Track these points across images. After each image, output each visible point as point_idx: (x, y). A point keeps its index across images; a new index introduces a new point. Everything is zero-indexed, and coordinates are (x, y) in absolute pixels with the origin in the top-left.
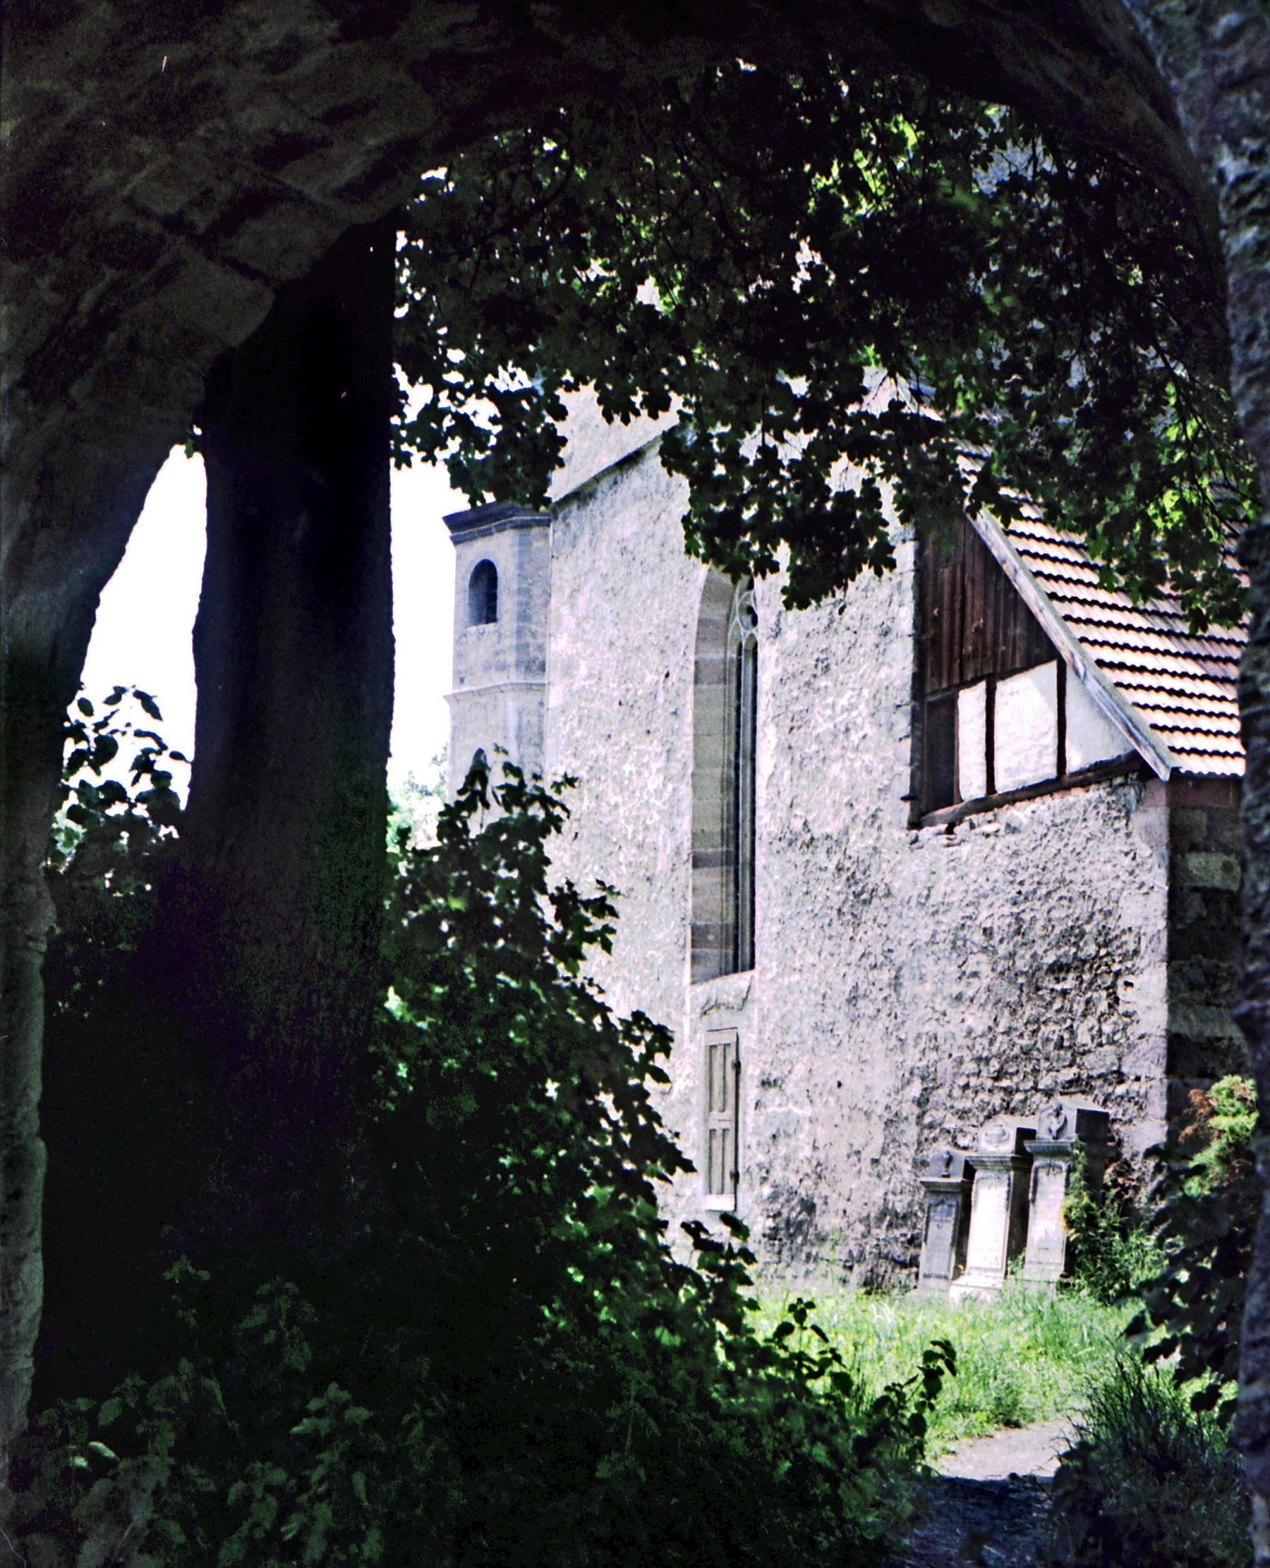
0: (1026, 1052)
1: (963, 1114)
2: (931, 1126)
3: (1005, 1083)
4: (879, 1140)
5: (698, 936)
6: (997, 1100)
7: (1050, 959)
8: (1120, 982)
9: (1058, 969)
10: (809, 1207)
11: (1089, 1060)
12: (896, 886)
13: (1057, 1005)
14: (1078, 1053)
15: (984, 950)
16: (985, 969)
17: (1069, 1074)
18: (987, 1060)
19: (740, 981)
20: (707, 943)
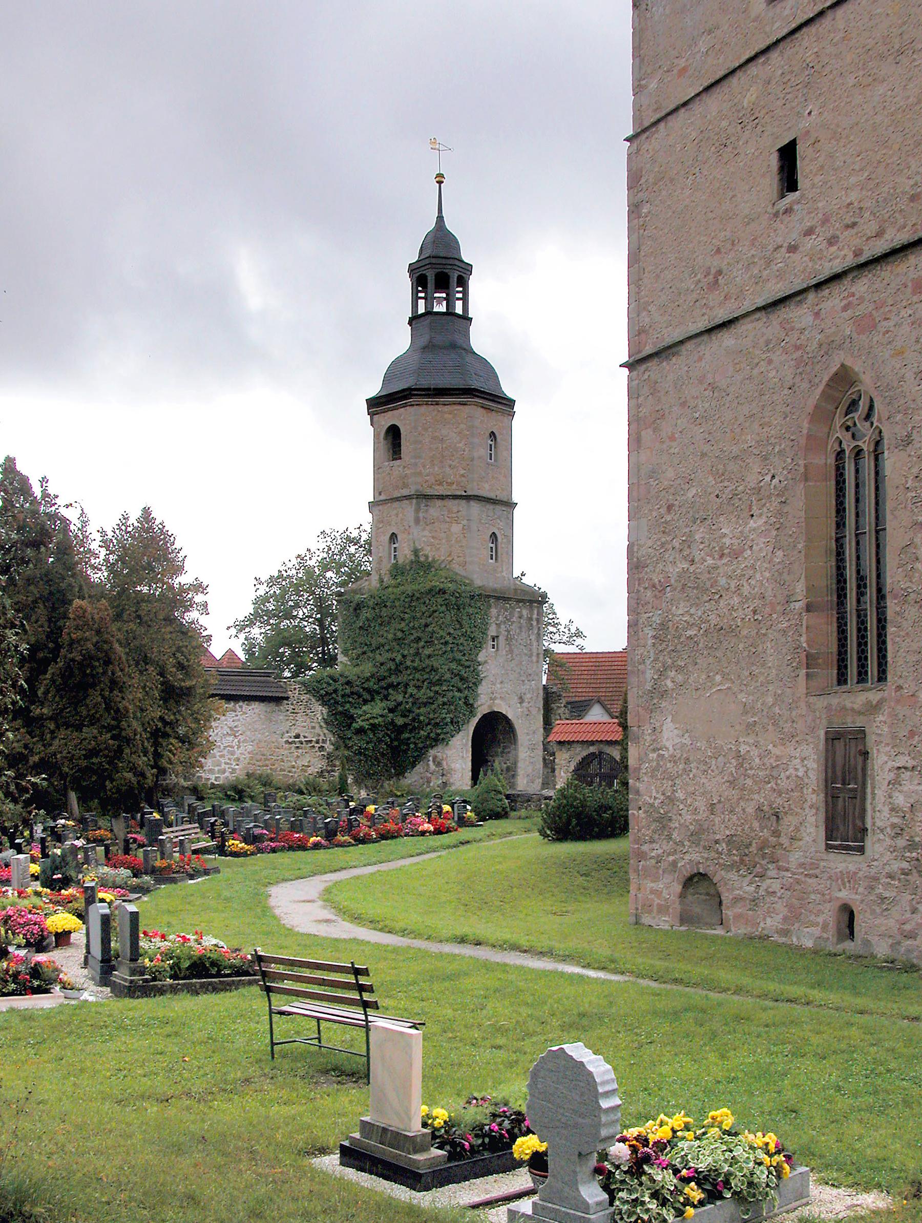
5: (811, 661)
19: (874, 696)
20: (817, 666)
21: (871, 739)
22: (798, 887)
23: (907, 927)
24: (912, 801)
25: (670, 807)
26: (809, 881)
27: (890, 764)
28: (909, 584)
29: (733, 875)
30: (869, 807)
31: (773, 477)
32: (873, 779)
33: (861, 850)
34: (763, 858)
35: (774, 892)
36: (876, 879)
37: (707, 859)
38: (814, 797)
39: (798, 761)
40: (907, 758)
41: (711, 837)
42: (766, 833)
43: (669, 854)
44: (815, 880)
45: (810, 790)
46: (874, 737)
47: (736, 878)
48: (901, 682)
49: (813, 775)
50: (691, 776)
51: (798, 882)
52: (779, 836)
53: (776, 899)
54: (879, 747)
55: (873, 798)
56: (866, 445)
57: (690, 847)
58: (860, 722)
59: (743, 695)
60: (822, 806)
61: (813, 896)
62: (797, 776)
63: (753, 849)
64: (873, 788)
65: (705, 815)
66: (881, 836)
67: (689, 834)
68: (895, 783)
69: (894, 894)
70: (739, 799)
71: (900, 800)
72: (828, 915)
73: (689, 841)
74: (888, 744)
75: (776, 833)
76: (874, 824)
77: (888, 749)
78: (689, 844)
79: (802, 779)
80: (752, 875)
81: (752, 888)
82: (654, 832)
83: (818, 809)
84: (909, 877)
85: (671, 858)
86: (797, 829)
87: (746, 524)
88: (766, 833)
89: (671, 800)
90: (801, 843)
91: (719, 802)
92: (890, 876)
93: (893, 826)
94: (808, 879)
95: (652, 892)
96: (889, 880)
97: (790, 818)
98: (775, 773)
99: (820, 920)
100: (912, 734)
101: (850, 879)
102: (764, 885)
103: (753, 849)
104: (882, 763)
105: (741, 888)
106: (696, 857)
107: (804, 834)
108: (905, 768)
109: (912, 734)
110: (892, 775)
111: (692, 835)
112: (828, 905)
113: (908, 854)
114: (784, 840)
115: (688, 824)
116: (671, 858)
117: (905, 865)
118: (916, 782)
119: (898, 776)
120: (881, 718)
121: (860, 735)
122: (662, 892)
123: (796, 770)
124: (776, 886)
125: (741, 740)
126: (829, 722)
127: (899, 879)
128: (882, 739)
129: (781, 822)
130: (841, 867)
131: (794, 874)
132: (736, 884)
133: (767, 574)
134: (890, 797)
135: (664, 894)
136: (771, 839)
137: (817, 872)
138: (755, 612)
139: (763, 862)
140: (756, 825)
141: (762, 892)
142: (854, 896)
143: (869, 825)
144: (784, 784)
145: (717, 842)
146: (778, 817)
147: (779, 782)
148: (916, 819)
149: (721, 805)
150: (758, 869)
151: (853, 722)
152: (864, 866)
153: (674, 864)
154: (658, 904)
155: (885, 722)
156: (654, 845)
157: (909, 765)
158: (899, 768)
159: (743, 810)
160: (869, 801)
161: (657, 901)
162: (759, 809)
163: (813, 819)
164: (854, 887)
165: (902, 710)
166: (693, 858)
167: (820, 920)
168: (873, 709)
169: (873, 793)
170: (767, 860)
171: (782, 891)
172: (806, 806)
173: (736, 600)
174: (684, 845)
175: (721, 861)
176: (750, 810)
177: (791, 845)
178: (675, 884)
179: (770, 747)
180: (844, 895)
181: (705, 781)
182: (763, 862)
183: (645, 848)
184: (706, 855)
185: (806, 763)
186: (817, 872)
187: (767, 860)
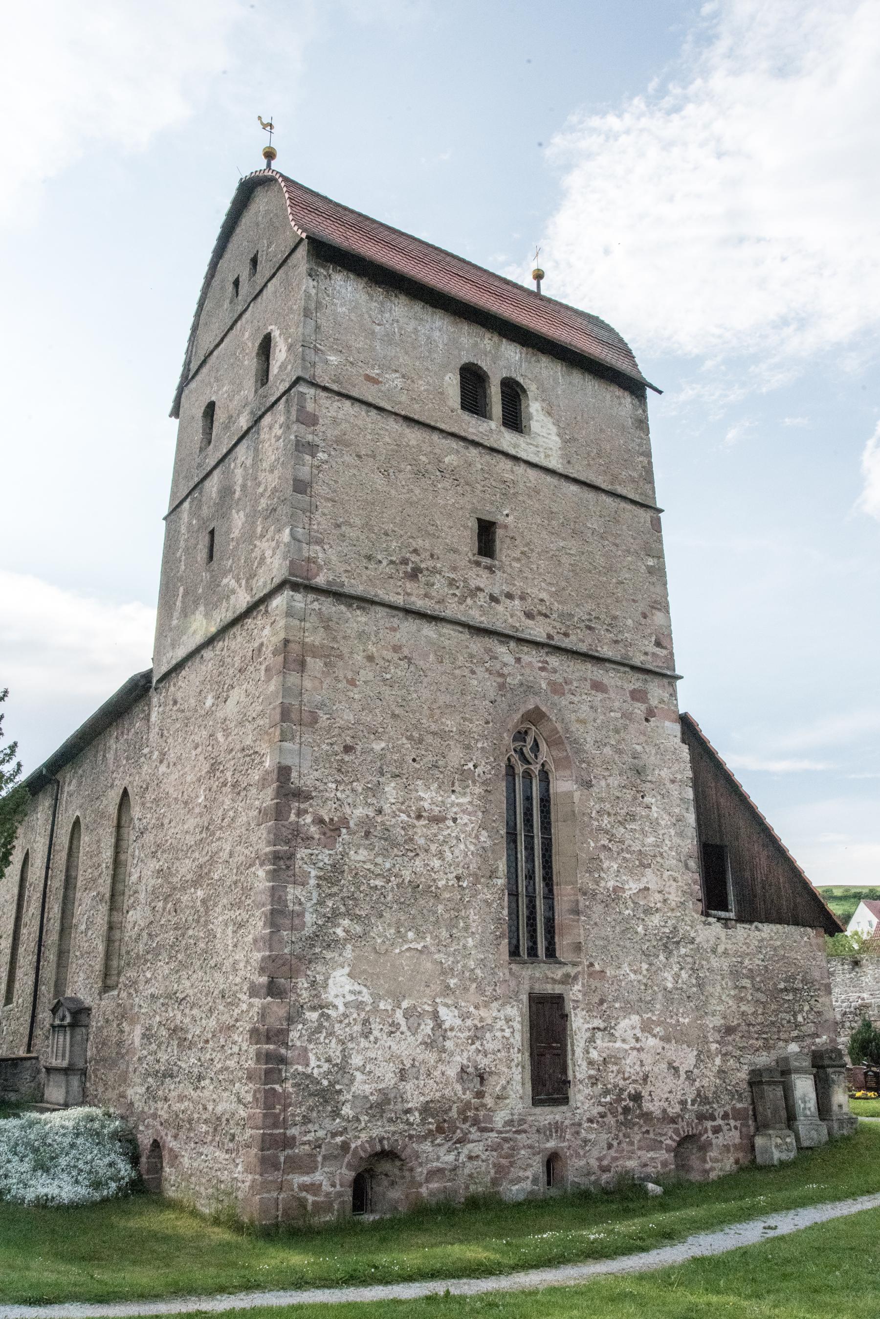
0: (773, 1023)
1: (741, 1049)
2: (725, 1054)
3: (765, 1036)
4: (691, 1059)
6: (760, 1043)
7: (782, 985)
8: (813, 999)
9: (786, 990)
10: (637, 1098)
11: (803, 1028)
12: (698, 940)
13: (786, 1005)
14: (797, 1026)
15: (748, 978)
16: (749, 986)
17: (795, 1033)
18: (754, 1025)
21: (569, 1006)
22: (506, 1146)
23: (605, 1163)
24: (604, 1055)
25: (339, 1076)
26: (519, 1137)
27: (586, 1026)
28: (596, 887)
29: (427, 1146)
30: (569, 1062)
31: (475, 766)
32: (572, 1039)
33: (565, 1101)
34: (465, 1120)
35: (477, 1156)
36: (580, 1125)
37: (394, 1133)
38: (520, 1057)
39: (504, 1022)
40: (600, 1021)
41: (399, 1107)
42: (468, 1096)
43: (334, 1135)
44: (524, 1135)
45: (516, 1049)
46: (571, 1004)
47: (430, 1149)
48: (592, 960)
49: (518, 1036)
50: (372, 1038)
51: (506, 1140)
52: (483, 1097)
53: (480, 1163)
54: (576, 1011)
55: (573, 1054)
56: (536, 769)
57: (369, 1121)
58: (558, 989)
59: (442, 955)
60: (528, 1063)
61: (523, 1152)
62: (503, 1037)
63: (454, 1113)
64: (572, 1045)
65: (393, 1082)
66: (581, 1087)
67: (368, 1105)
68: (592, 1040)
69: (594, 1136)
70: (437, 1062)
71: (594, 1055)
72: (537, 1166)
73: (367, 1114)
74: (583, 1009)
75: (480, 1095)
76: (575, 1077)
77: (584, 1013)
78: (367, 1118)
79: (508, 1039)
80: (450, 1143)
81: (451, 1158)
82: (311, 1109)
83: (523, 1067)
84: (605, 1119)
85: (339, 1139)
86: (504, 1088)
87: (449, 797)
88: (468, 1096)
89: (342, 1067)
90: (507, 1101)
91: (413, 1066)
92: (590, 1121)
93: (590, 1077)
94: (516, 1136)
95: (304, 1187)
96: (590, 1124)
97: (496, 1078)
98: (479, 1035)
99: (529, 1173)
100: (602, 1001)
101: (557, 1128)
102: (465, 1151)
103: (454, 1113)
104: (580, 1023)
105: (438, 1158)
106: (377, 1132)
107: (511, 1093)
108: (598, 1029)
109: (602, 1001)
110: (588, 1034)
111: (371, 1108)
112: (538, 1158)
113: (603, 1100)
114: (489, 1101)
115: (367, 1094)
116: (339, 1139)
117: (601, 1109)
118: (606, 1040)
119: (594, 1036)
120: (577, 987)
121: (558, 1001)
122: (321, 1185)
123: (503, 1030)
124: (477, 1148)
125: (438, 1000)
126: (531, 988)
127: (598, 1122)
128: (579, 1004)
129: (485, 1083)
130: (550, 1118)
131: (500, 1132)
132: (432, 1156)
133: (472, 848)
134: (588, 1053)
135: (324, 1188)
136: (473, 1101)
137: (525, 1126)
138: (458, 878)
139: (464, 1126)
140: (458, 1087)
141: (463, 1158)
142: (562, 1145)
143: (570, 1078)
144: (490, 1046)
145: (408, 1111)
146: (482, 1079)
147: (485, 1042)
148: (608, 1070)
149: (415, 1070)
150: (459, 1134)
151: (553, 989)
152: (569, 1114)
153: (345, 1147)
154: (314, 1203)
155: (579, 991)
156: (310, 1126)
157: (602, 1026)
158: (594, 1029)
159: (443, 1074)
160: (570, 1057)
161: (311, 1198)
162: (463, 1070)
163: (520, 1076)
164: (561, 1137)
165: (594, 983)
166: (368, 1134)
167: (529, 1173)
168: (568, 980)
169: (573, 1051)
170: (468, 1124)
171: (487, 1153)
172: (513, 1064)
173: (436, 863)
174: (358, 1120)
175: (413, 1132)
176: (452, 1072)
177: (496, 1103)
178: (344, 1170)
179: (472, 1009)
180: (551, 1144)
181: (391, 1043)
182: (464, 1126)
183: (293, 1131)
184: (392, 1128)
185: (510, 1025)
186: (525, 1126)
187: (468, 1124)
